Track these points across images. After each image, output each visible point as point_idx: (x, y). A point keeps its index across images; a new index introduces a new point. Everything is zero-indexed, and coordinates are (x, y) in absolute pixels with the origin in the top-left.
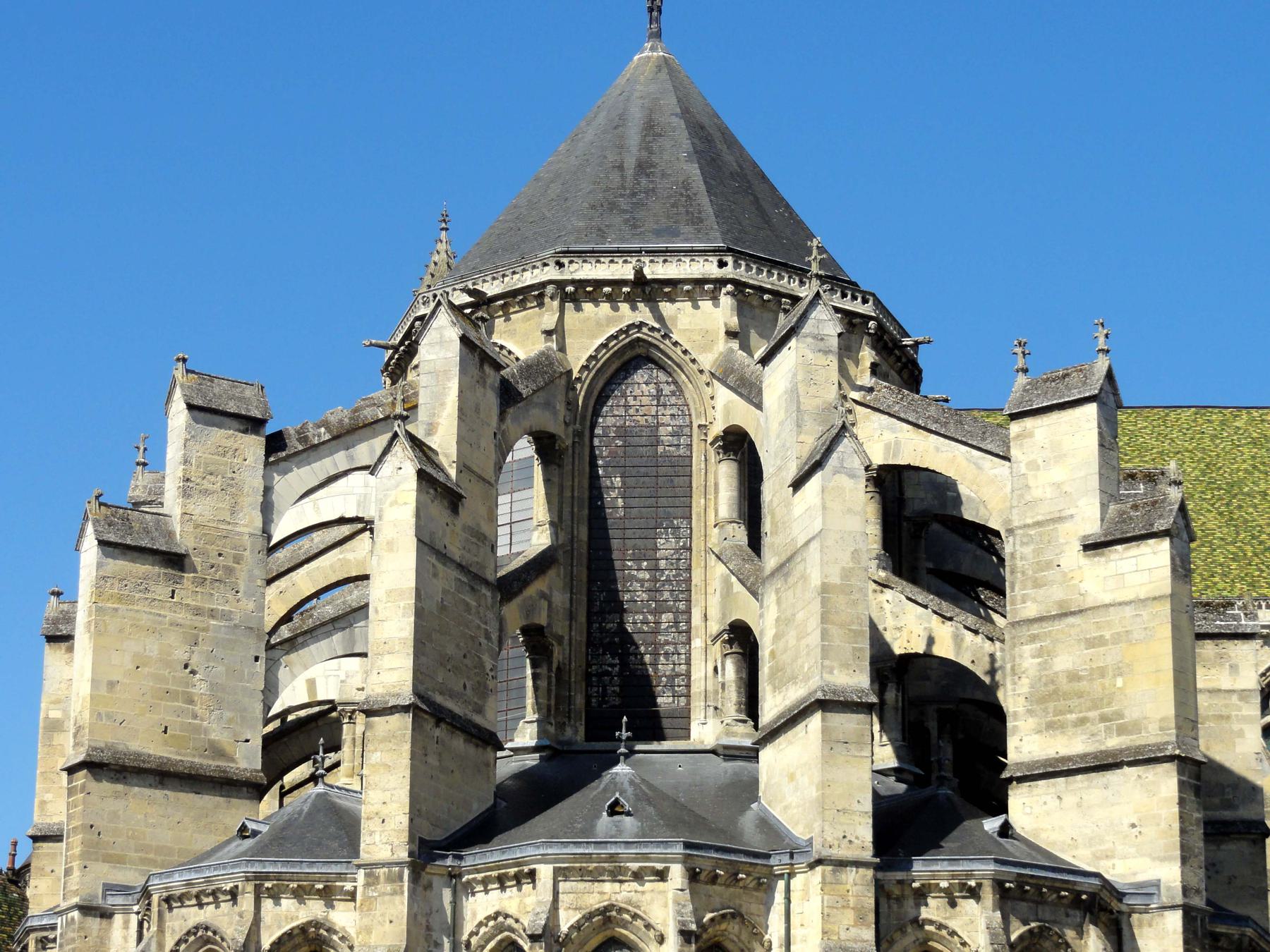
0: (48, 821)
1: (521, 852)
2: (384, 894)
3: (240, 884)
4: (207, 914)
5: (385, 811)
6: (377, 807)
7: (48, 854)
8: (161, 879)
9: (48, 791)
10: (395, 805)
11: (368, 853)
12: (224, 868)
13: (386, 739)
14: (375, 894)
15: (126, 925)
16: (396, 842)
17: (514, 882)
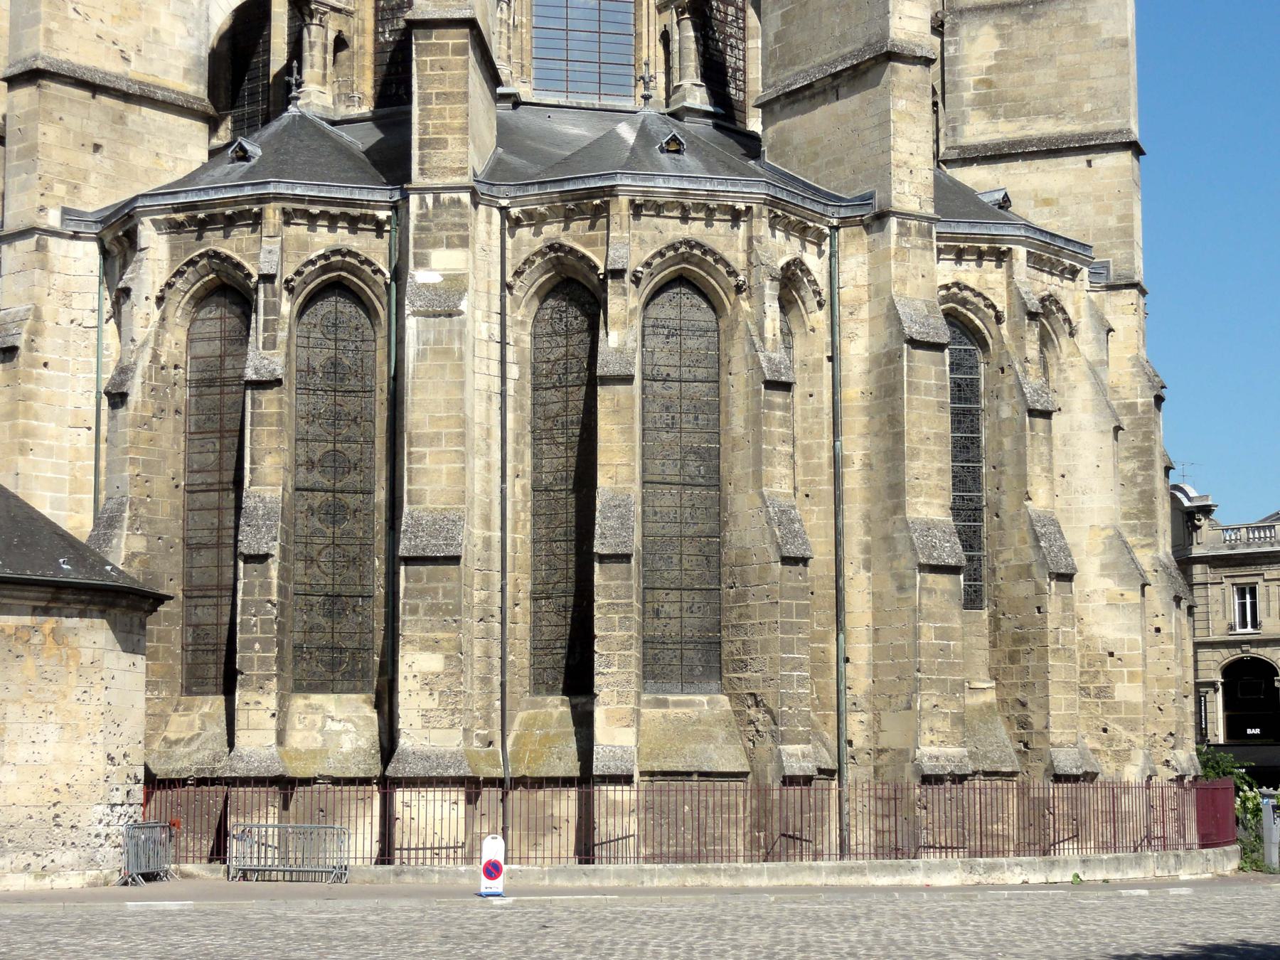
0: (54, 55)
1: (996, 230)
2: (915, 247)
3: (754, 205)
4: (695, 230)
5: (913, 161)
6: (905, 157)
7: (56, 97)
8: (634, 180)
9: (53, 20)
10: (921, 159)
11: (899, 201)
12: (732, 185)
13: (912, 88)
14: (908, 246)
15: (489, 216)
16: (924, 197)
17: (975, 257)
